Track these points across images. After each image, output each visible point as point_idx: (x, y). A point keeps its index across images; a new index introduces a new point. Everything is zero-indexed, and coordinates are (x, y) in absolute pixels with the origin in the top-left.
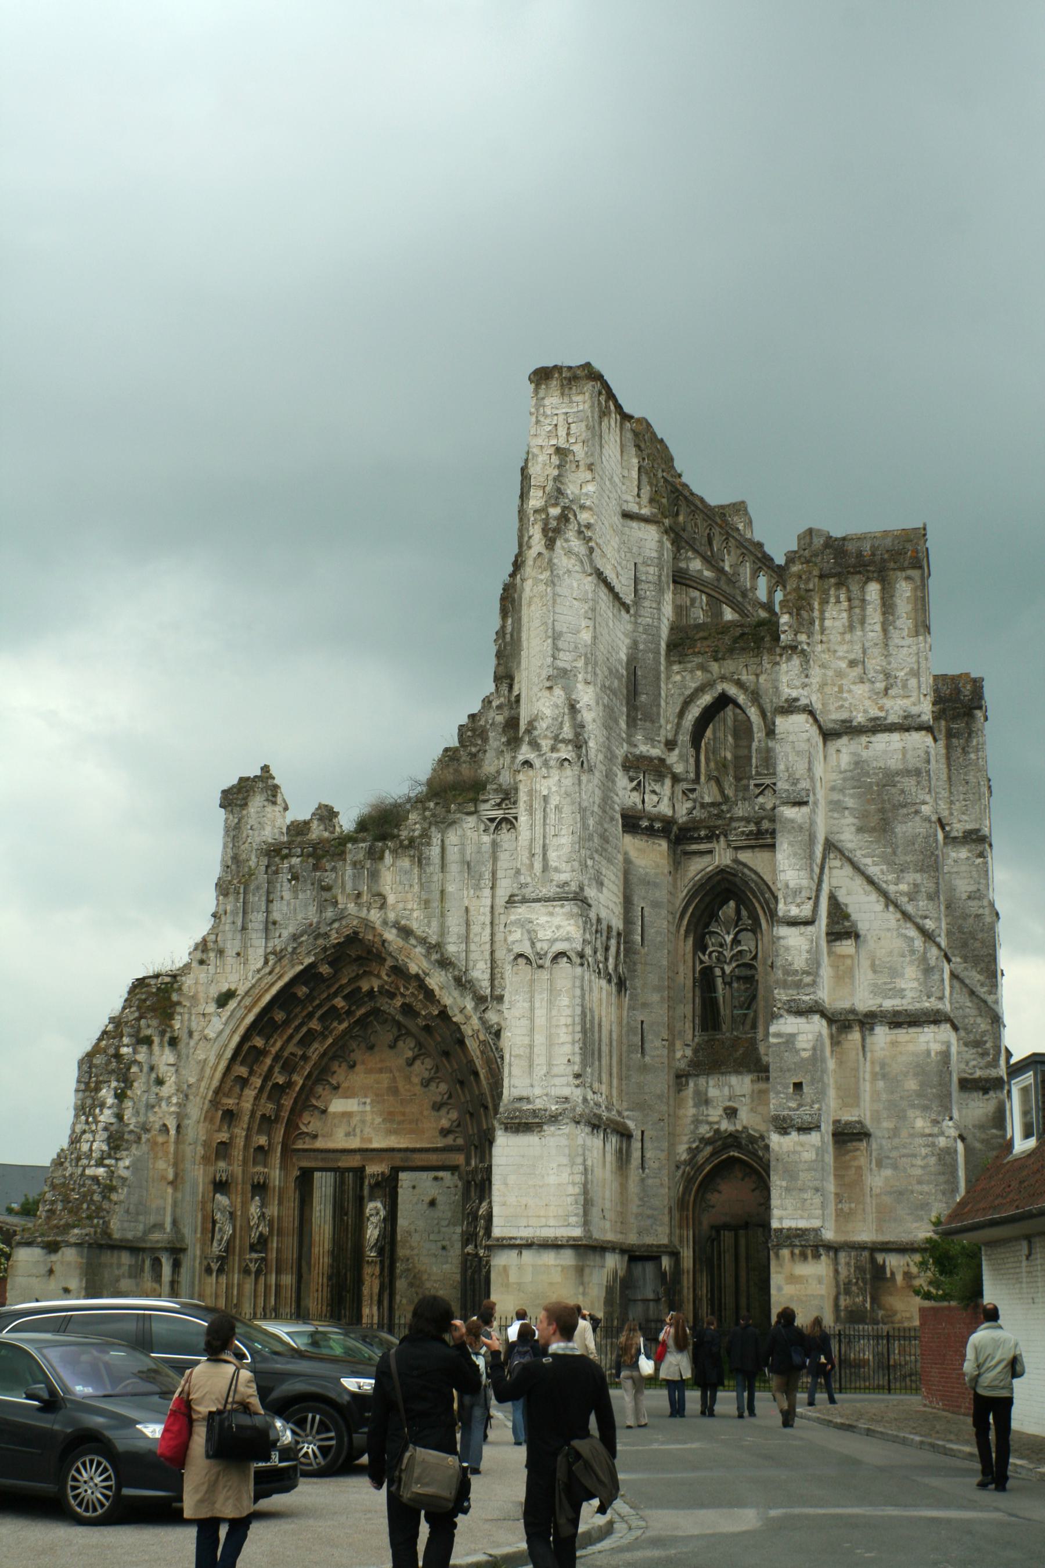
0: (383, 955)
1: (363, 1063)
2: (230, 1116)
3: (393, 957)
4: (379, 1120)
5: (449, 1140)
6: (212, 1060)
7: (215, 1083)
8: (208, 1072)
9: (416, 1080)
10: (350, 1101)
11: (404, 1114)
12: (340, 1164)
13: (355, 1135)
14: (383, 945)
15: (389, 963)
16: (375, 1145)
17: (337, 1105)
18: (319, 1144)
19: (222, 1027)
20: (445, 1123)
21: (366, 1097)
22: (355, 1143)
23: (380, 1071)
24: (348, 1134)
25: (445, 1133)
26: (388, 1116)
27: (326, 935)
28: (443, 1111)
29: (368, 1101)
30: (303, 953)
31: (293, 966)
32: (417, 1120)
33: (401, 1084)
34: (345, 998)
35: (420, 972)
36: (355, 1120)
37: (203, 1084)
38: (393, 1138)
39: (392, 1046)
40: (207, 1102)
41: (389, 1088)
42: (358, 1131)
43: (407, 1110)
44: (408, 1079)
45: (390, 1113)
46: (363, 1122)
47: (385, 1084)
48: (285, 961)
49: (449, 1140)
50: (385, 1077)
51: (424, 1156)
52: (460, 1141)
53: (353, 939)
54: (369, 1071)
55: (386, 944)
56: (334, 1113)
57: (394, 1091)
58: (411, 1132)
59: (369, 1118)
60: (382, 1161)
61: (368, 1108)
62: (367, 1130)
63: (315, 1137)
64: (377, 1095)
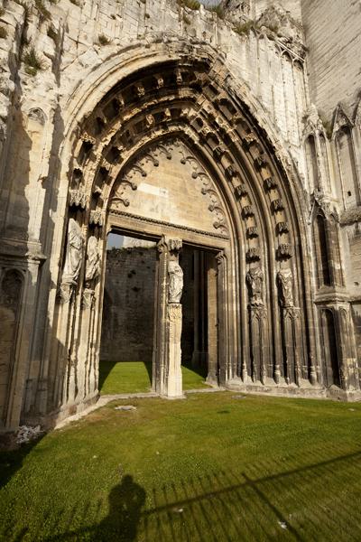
0: (219, 89)
1: (163, 166)
2: (87, 147)
3: (228, 90)
4: (174, 206)
5: (218, 231)
6: (86, 86)
7: (89, 106)
8: (81, 92)
9: (199, 189)
10: (154, 187)
11: (191, 207)
12: (145, 230)
13: (157, 212)
14: (225, 80)
15: (223, 95)
16: (171, 222)
17: (143, 187)
18: (129, 210)
19: (100, 62)
20: (215, 220)
21: (165, 188)
22: (158, 217)
23: (175, 175)
24: (152, 210)
25: (215, 226)
26: (181, 206)
27: (191, 49)
28: (215, 212)
29: (167, 192)
30: (174, 50)
31: (165, 54)
32: (199, 214)
33: (188, 187)
34: (171, 111)
35: (251, 107)
36: (157, 202)
37: (74, 102)
38: (184, 220)
39: (183, 163)
40: (75, 123)
41: (181, 188)
42: (159, 209)
43: (193, 205)
44: (193, 185)
45: (181, 204)
46: (164, 205)
47: (178, 184)
48: (160, 45)
49: (218, 231)
50: (178, 181)
51: (205, 237)
52: (224, 233)
53: (204, 66)
54: (168, 173)
55: (229, 79)
56: (141, 192)
57: (185, 191)
58: (195, 220)
59: (168, 203)
60: (177, 234)
61: (167, 196)
62: (165, 211)
63: (127, 206)
64: (173, 189)
